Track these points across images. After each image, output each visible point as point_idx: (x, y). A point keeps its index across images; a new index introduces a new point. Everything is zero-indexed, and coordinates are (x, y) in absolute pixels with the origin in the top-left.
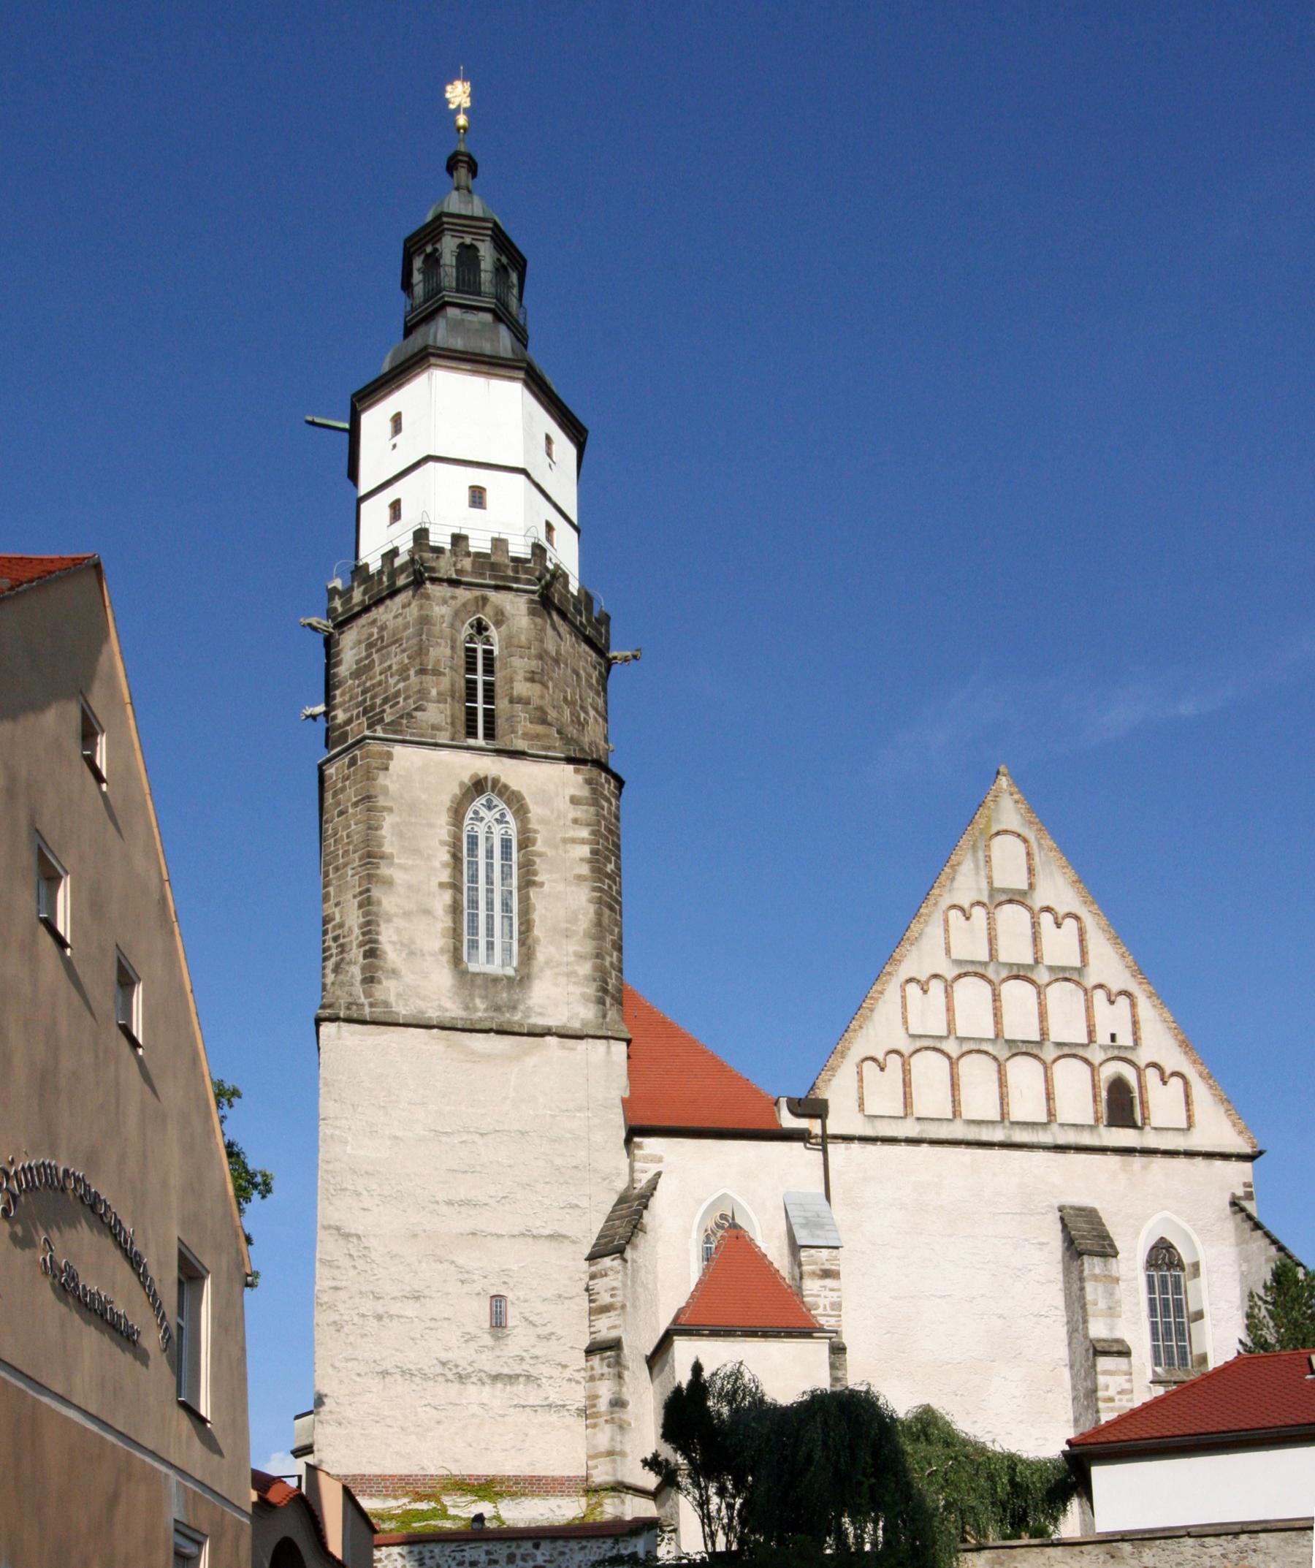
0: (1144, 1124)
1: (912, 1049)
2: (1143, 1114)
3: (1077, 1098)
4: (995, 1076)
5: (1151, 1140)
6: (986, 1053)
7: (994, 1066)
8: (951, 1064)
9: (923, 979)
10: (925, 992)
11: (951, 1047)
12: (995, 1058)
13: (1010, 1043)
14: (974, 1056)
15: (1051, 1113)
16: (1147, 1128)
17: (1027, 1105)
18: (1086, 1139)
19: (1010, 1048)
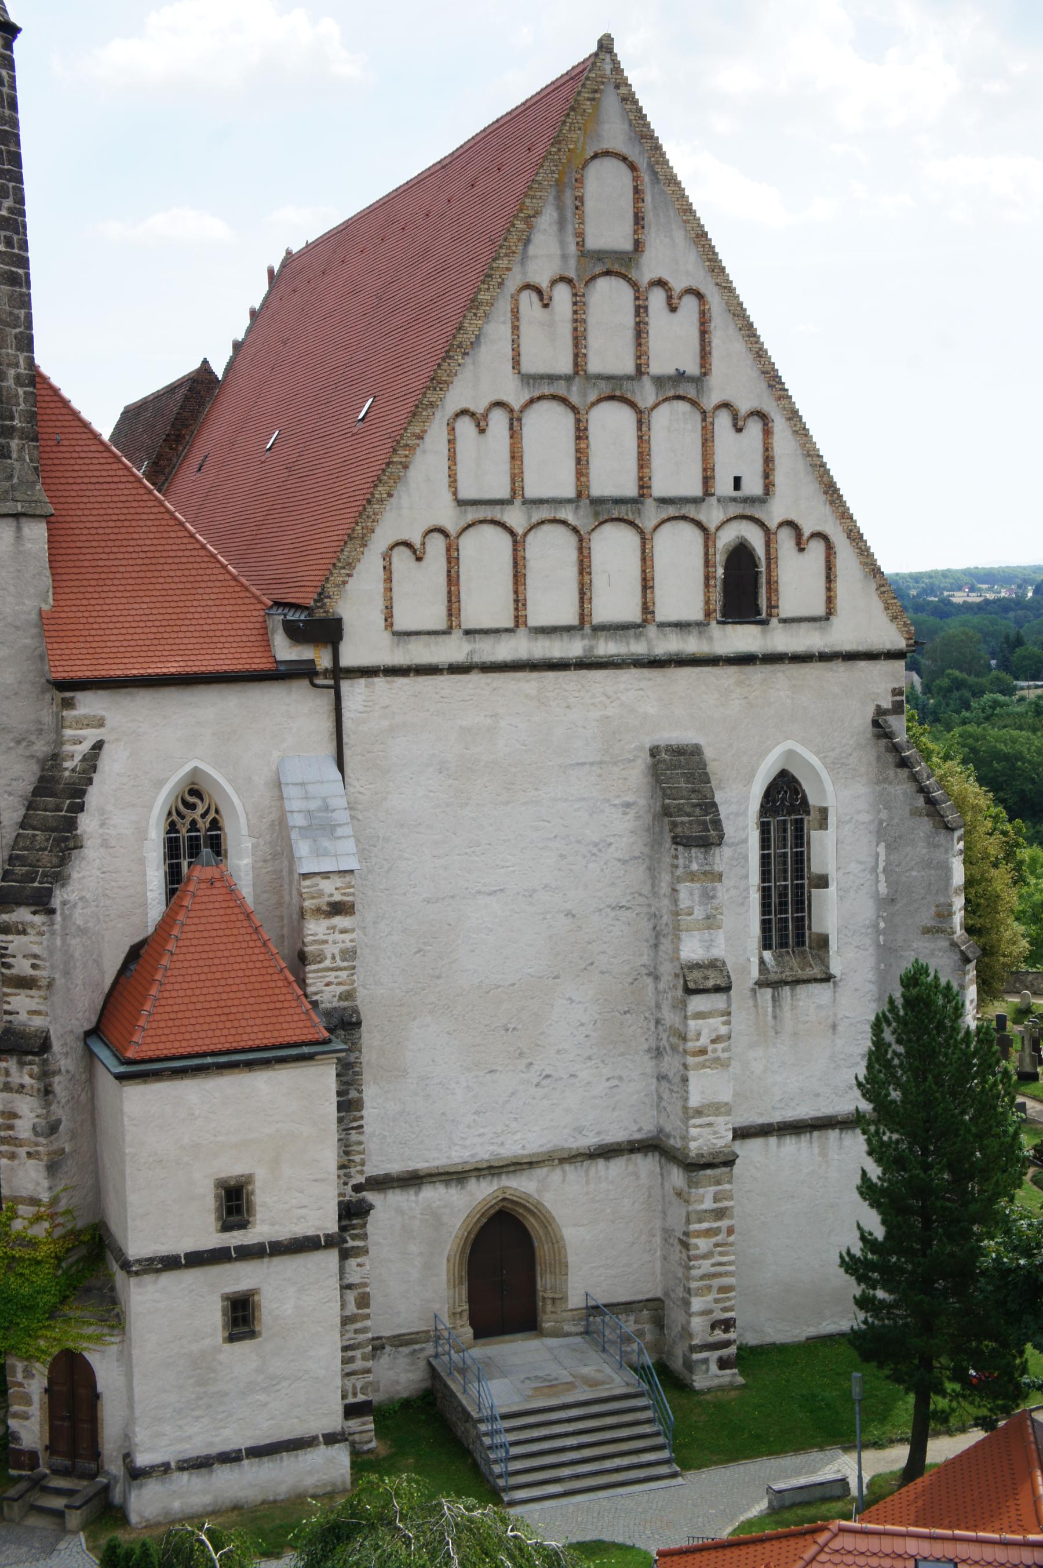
0: (770, 615)
1: (463, 524)
2: (769, 599)
3: (683, 582)
4: (573, 555)
5: (781, 640)
6: (563, 522)
7: (572, 540)
8: (515, 542)
9: (479, 408)
10: (482, 431)
11: (516, 518)
12: (575, 530)
13: (597, 502)
14: (547, 528)
15: (647, 609)
16: (774, 621)
17: (615, 602)
18: (691, 645)
19: (596, 514)
